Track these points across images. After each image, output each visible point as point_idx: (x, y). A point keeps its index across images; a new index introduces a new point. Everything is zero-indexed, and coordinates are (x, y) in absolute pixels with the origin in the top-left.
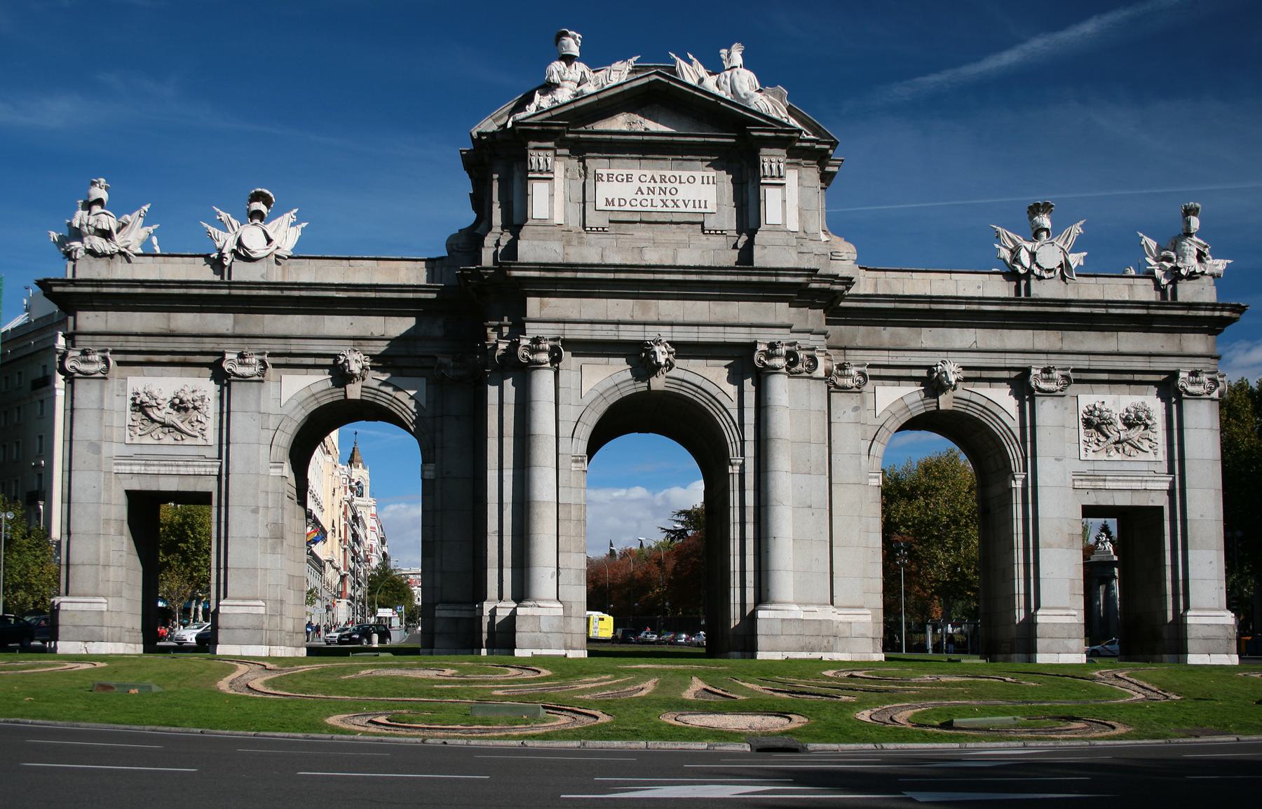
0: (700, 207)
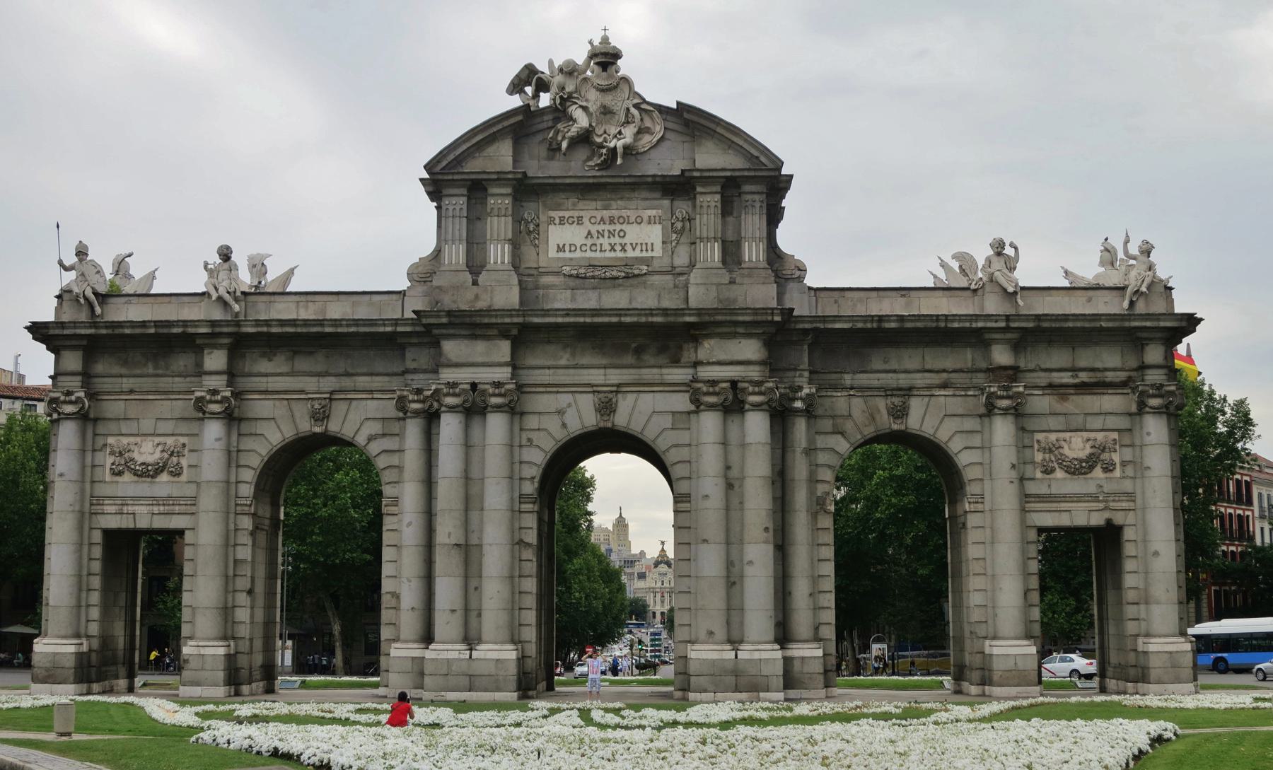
0: (647, 250)
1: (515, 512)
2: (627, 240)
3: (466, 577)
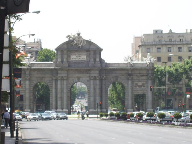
1: (67, 93)
2: (81, 57)
3: (61, 101)
